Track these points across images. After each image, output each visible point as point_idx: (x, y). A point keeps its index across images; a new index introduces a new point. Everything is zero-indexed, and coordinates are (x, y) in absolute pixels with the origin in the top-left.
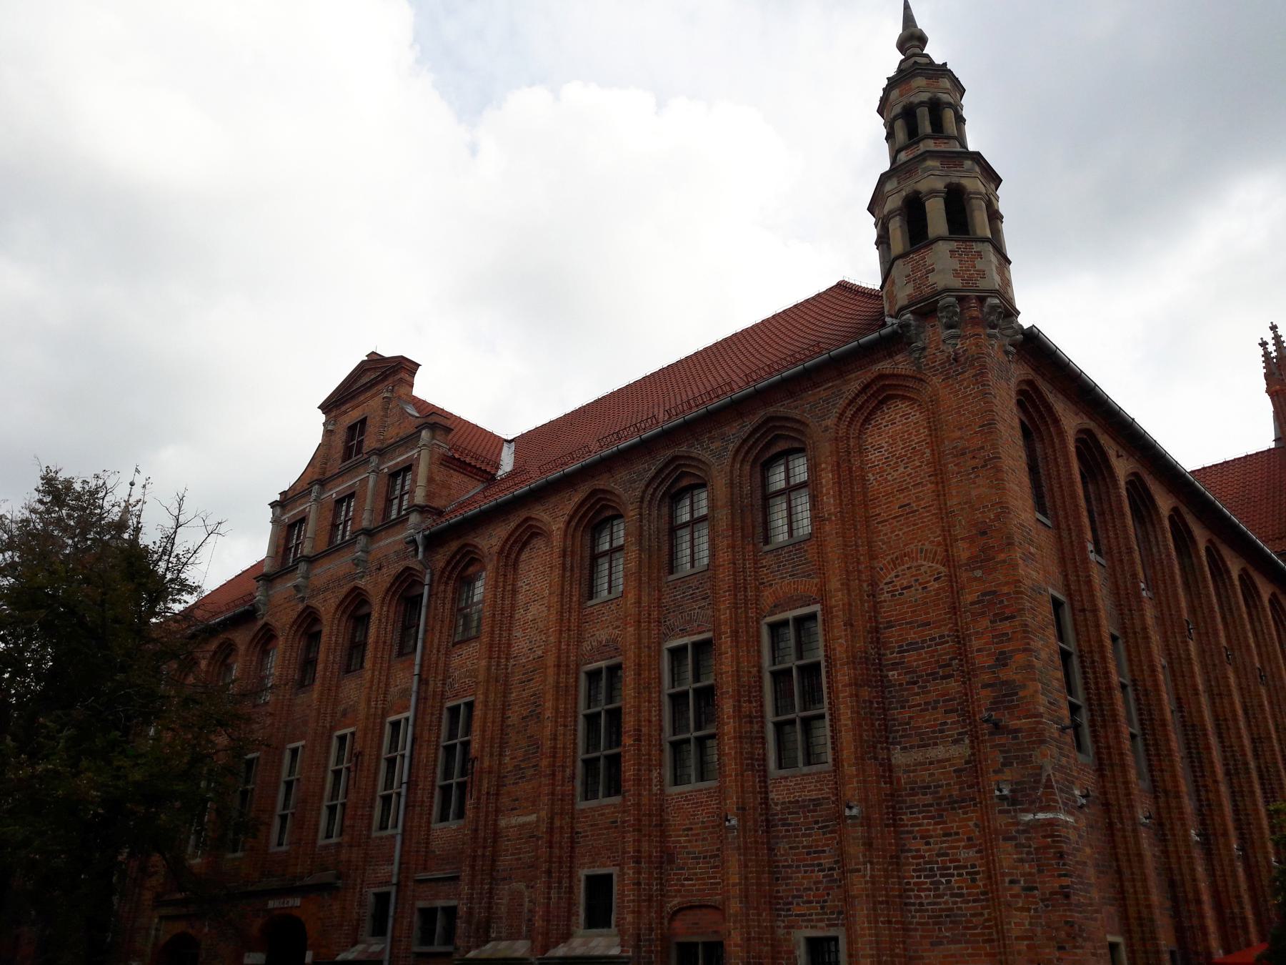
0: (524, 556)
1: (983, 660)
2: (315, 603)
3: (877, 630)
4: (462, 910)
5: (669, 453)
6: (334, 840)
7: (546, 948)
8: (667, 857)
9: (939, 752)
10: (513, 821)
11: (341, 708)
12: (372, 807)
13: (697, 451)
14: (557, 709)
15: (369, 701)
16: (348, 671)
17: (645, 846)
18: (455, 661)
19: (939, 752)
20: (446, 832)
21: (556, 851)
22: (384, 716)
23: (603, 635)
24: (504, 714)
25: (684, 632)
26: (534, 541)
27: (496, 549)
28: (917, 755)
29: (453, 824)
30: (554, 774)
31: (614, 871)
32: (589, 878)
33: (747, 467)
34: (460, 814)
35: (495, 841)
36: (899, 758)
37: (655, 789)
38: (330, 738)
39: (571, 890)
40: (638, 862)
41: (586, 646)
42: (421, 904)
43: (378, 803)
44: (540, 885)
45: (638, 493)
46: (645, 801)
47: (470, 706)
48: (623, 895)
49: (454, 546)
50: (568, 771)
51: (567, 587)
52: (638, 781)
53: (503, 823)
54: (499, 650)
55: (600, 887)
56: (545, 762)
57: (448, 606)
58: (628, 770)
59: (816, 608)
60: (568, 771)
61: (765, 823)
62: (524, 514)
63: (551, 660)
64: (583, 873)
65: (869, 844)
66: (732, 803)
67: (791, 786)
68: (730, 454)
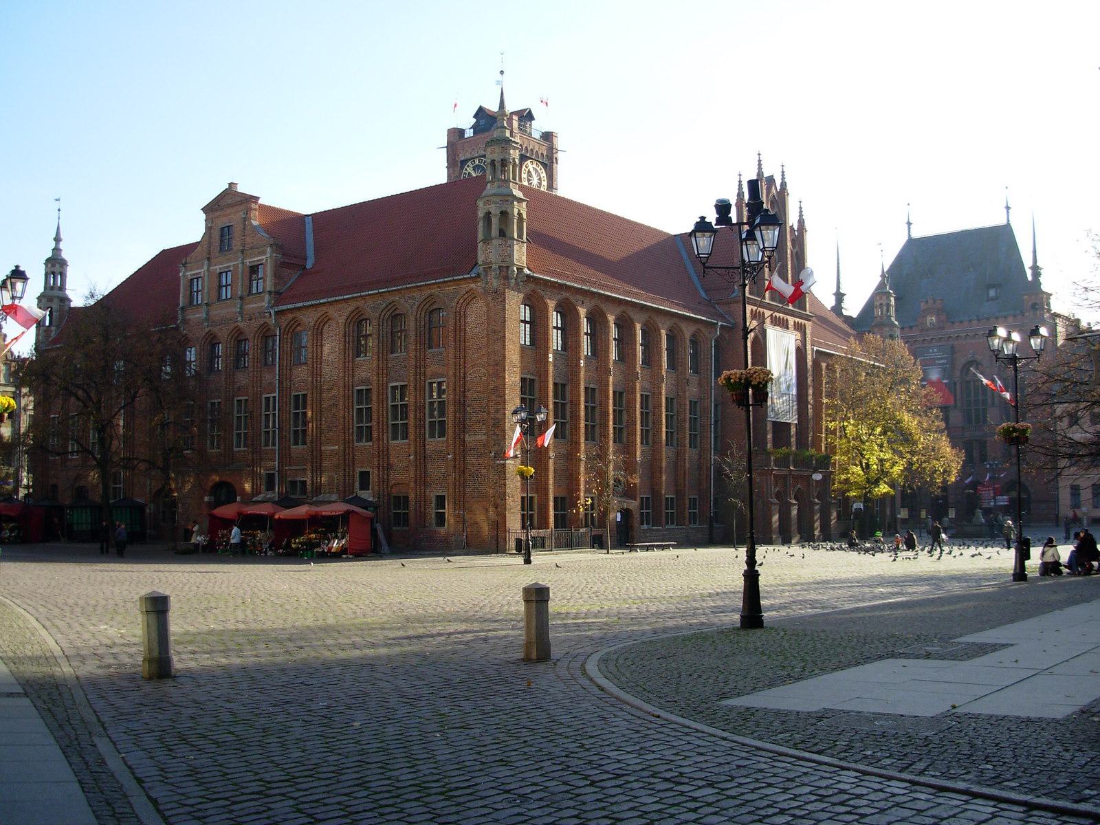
0: (325, 329)
1: (492, 410)
2: (215, 329)
3: (464, 392)
4: (309, 482)
5: (392, 298)
6: (242, 449)
7: (345, 497)
8: (390, 466)
9: (479, 437)
10: (328, 448)
11: (236, 386)
12: (260, 435)
13: (402, 301)
14: (344, 405)
15: (253, 387)
16: (237, 367)
17: (381, 464)
18: (295, 372)
19: (479, 437)
20: (297, 450)
21: (347, 462)
22: (261, 395)
23: (364, 375)
24: (320, 403)
25: (397, 380)
26: (330, 322)
27: (312, 324)
28: (473, 438)
29: (300, 447)
30: (345, 433)
31: (371, 470)
32: (361, 472)
33: (423, 313)
34: (304, 443)
35: (321, 456)
36: (467, 438)
37: (385, 441)
38: (233, 400)
39: (353, 476)
40: (379, 468)
41: (356, 379)
42: (289, 479)
43: (263, 434)
44: (341, 474)
45: (377, 314)
46: (381, 446)
47: (305, 396)
48: (373, 479)
49: (290, 316)
50: (351, 431)
51: (347, 352)
52: (379, 439)
53: (323, 448)
54: (316, 373)
55: (365, 476)
56: (341, 427)
57: (289, 346)
58: (375, 435)
59: (445, 379)
60: (351, 431)
61: (422, 456)
62: (324, 309)
63: (341, 385)
64: (358, 470)
65: (455, 467)
66: (412, 449)
67: (434, 443)
68: (416, 307)
